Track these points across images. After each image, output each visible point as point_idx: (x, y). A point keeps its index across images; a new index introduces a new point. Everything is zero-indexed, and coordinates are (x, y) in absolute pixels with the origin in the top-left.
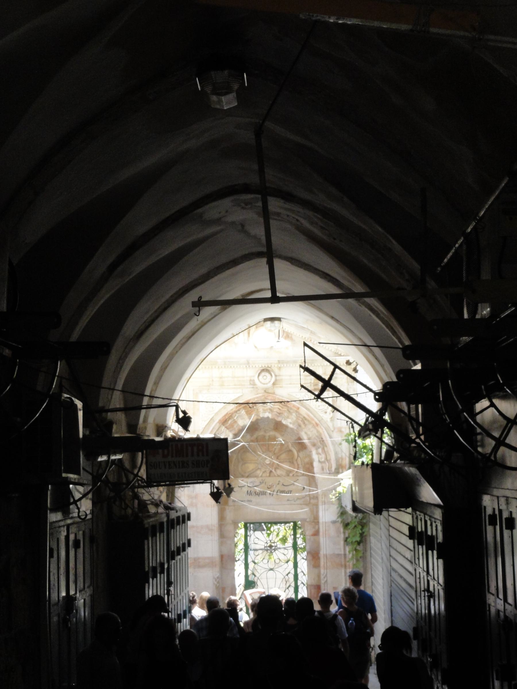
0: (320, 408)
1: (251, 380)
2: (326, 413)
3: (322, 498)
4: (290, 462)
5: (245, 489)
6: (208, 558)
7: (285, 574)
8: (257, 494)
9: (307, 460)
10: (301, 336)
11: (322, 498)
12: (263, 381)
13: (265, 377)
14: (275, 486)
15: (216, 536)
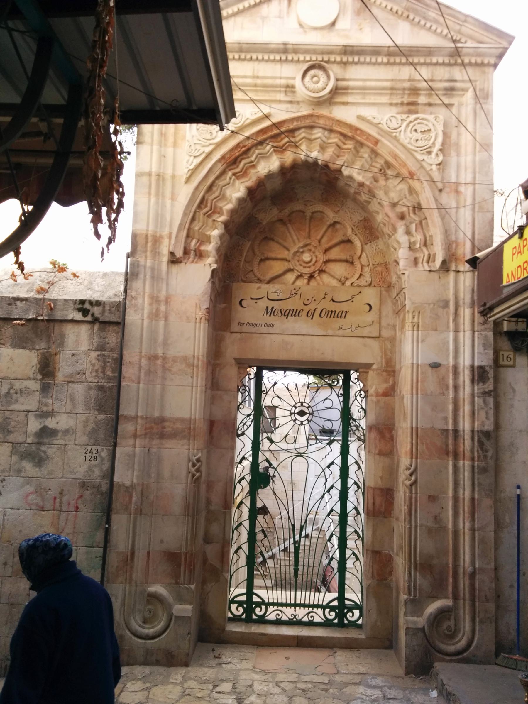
0: (420, 143)
2: (430, 153)
3: (414, 318)
4: (347, 261)
5: (263, 304)
6: (182, 420)
7: (325, 464)
8: (285, 314)
9: (378, 260)
10: (389, 8)
11: (414, 318)
12: (312, 86)
13: (315, 79)
15: (199, 379)
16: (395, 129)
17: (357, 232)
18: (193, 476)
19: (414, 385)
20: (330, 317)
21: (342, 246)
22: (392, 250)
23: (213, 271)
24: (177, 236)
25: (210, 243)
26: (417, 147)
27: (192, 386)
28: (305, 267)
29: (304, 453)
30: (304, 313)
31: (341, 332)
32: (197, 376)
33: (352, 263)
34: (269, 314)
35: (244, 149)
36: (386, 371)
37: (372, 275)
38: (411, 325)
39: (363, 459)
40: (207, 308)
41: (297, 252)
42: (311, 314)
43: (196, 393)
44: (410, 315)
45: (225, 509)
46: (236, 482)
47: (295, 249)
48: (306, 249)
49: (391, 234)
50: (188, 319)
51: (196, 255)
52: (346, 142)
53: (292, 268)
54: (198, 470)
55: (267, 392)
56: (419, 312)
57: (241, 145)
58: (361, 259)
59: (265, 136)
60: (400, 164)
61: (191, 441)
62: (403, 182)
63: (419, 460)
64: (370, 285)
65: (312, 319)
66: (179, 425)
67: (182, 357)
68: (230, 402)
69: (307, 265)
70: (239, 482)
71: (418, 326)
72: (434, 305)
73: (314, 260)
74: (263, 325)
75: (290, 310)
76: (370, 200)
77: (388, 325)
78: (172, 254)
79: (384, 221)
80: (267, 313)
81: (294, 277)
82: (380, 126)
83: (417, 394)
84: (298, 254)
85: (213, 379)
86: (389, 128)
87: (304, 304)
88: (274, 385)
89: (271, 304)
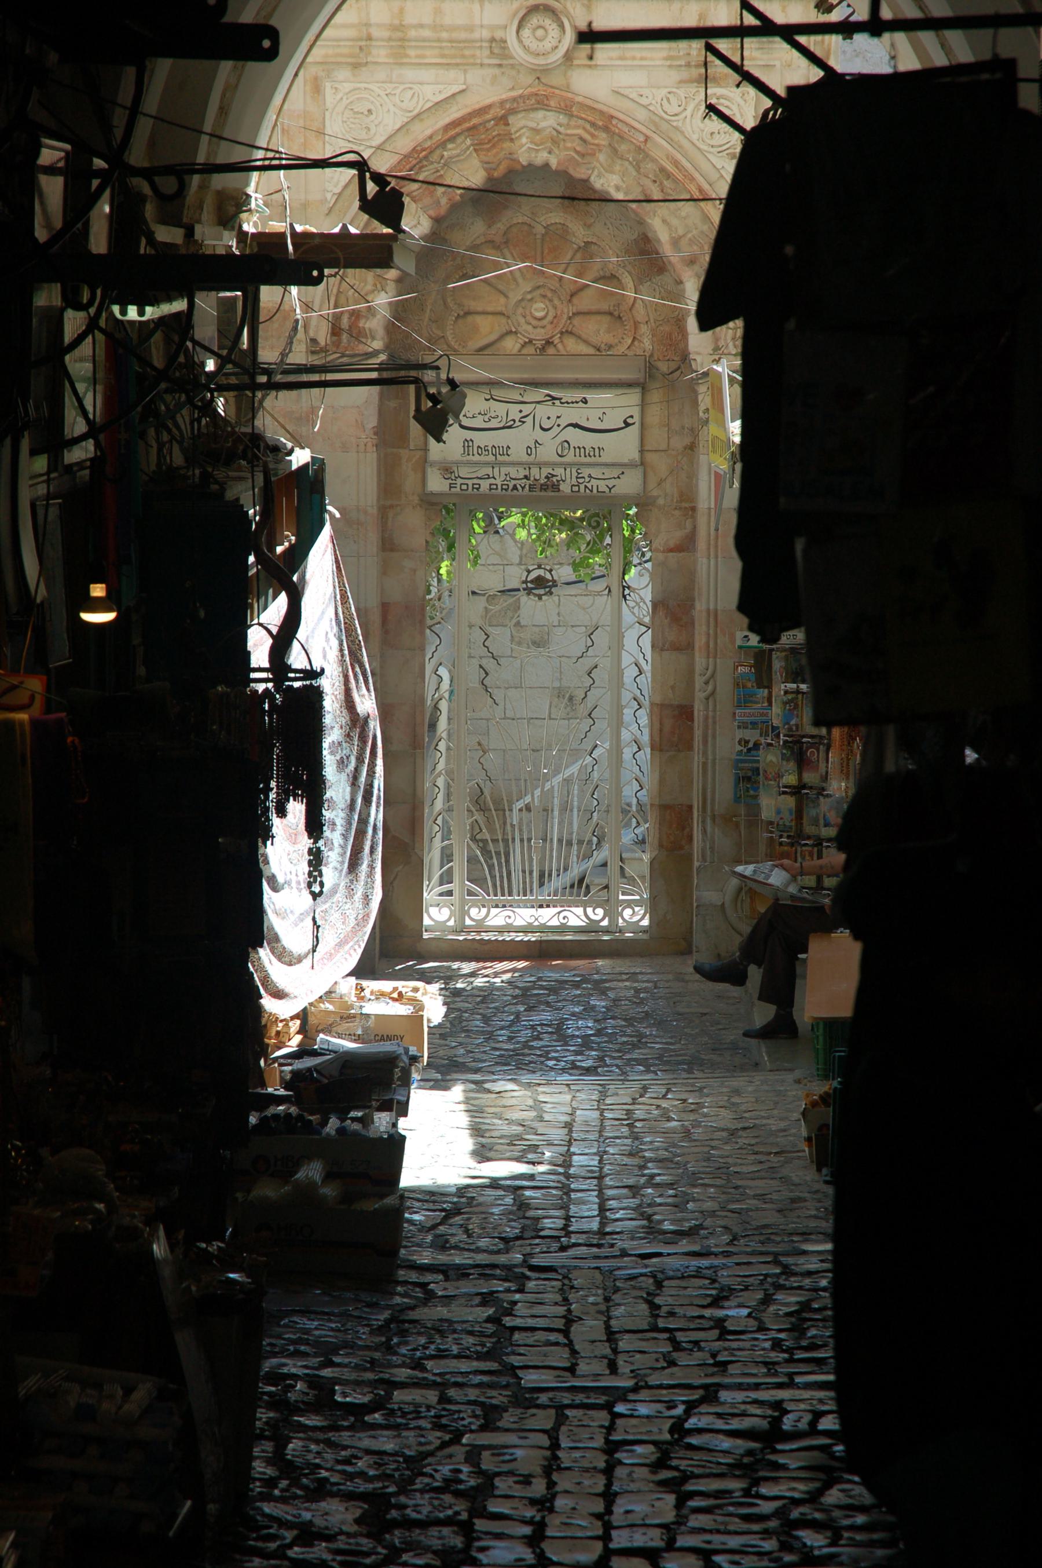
1: (493, 40)
4: (611, 314)
12: (534, 45)
13: (540, 33)
16: (676, 115)
19: (712, 542)
35: (424, 153)
36: (680, 508)
39: (649, 657)
41: (522, 300)
45: (415, 748)
52: (596, 133)
57: (419, 148)
58: (634, 312)
59: (457, 130)
63: (718, 660)
68: (415, 571)
69: (541, 323)
77: (683, 428)
82: (651, 108)
83: (716, 557)
84: (523, 304)
85: (383, 531)
86: (666, 113)
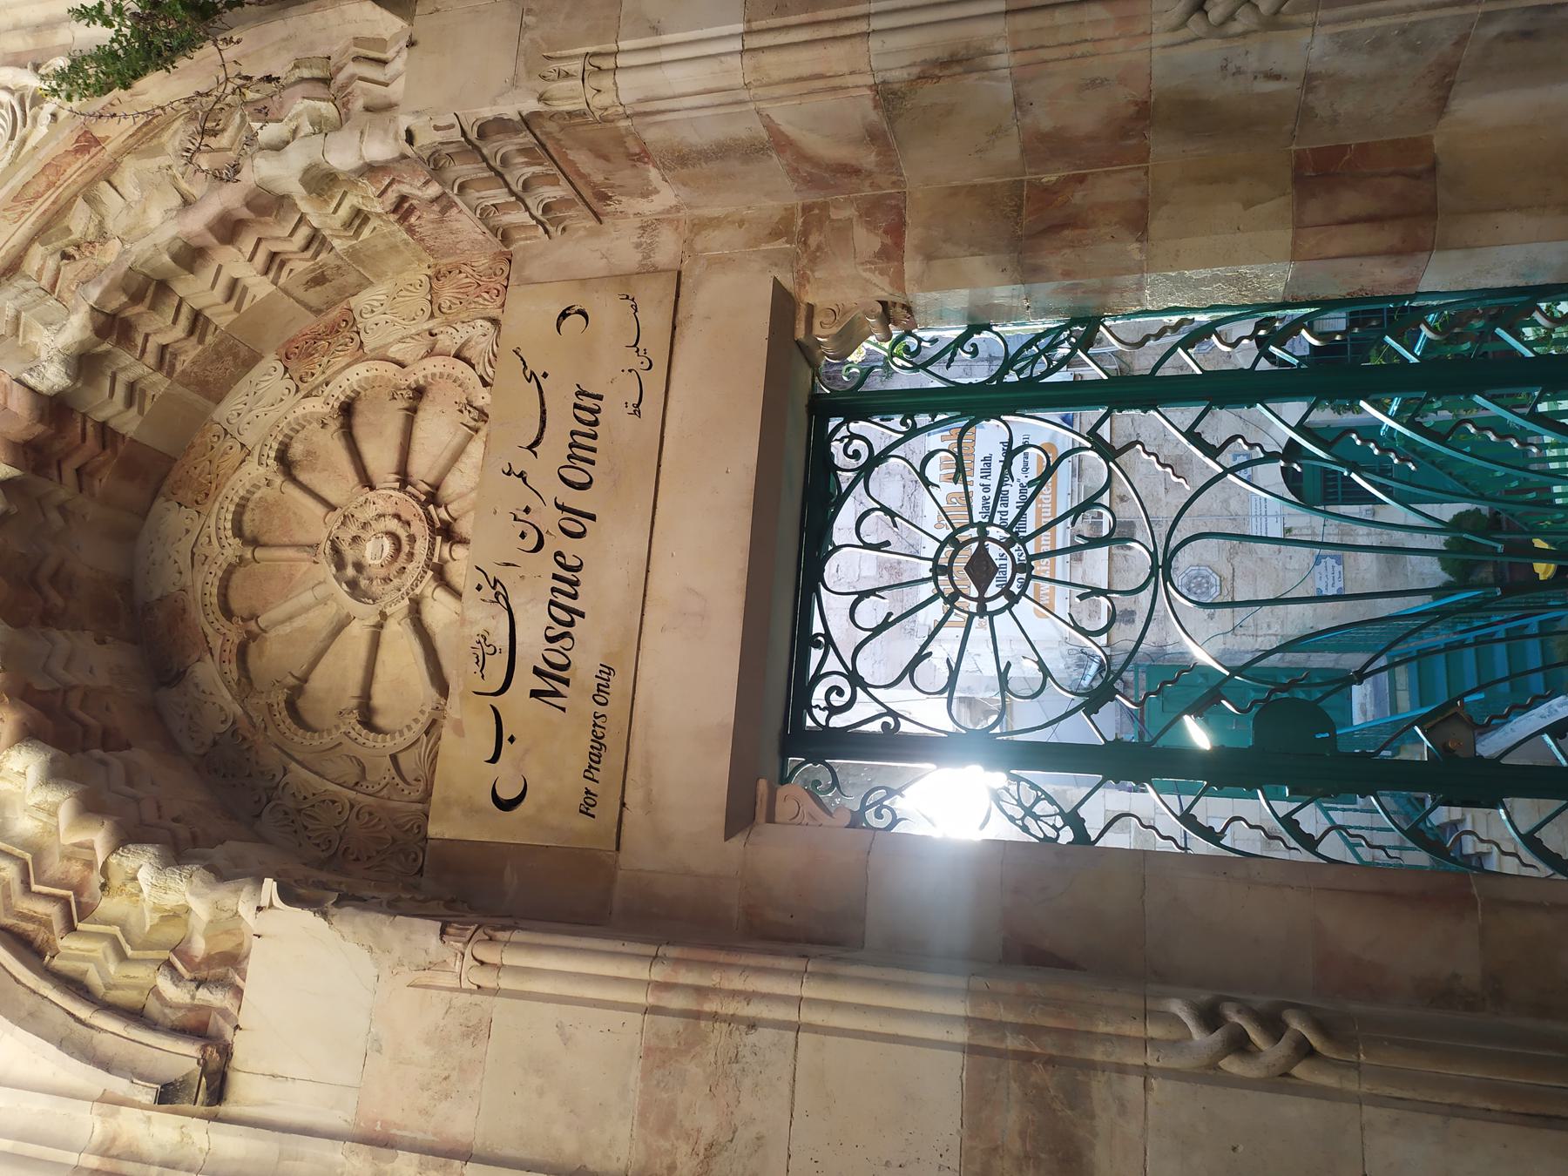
4: (412, 412)
6: (977, 1100)
11: (568, 75)
14: (535, 503)
15: (770, 989)
17: (321, 379)
18: (1305, 1051)
20: (593, 450)
21: (360, 431)
22: (366, 233)
23: (289, 896)
24: (105, 1064)
25: (188, 910)
26: (12, 138)
27: (798, 1028)
28: (411, 555)
29: (1153, 555)
30: (571, 548)
31: (651, 407)
32: (748, 996)
33: (419, 392)
34: (560, 687)
36: (805, 233)
37: (463, 316)
38: (592, 82)
40: (443, 932)
41: (353, 585)
42: (577, 522)
43: (834, 1005)
44: (558, 88)
46: (1304, 856)
47: (342, 591)
48: (350, 554)
49: (304, 232)
50: (477, 1031)
51: (221, 983)
53: (406, 602)
54: (1273, 1026)
55: (890, 712)
56: (549, 58)
60: (51, 185)
61: (1098, 1055)
62: (116, 180)
64: (495, 322)
65: (592, 517)
66: (1010, 1120)
67: (646, 1074)
69: (406, 548)
70: (1310, 843)
71: (595, 55)
72: (529, 11)
73: (394, 525)
74: (601, 710)
75: (552, 603)
76: (185, 310)
77: (638, 246)
78: (168, 1094)
79: (261, 257)
80: (556, 694)
81: (440, 594)
84: (363, 583)
87: (536, 550)
88: (865, 687)
89: (525, 680)
